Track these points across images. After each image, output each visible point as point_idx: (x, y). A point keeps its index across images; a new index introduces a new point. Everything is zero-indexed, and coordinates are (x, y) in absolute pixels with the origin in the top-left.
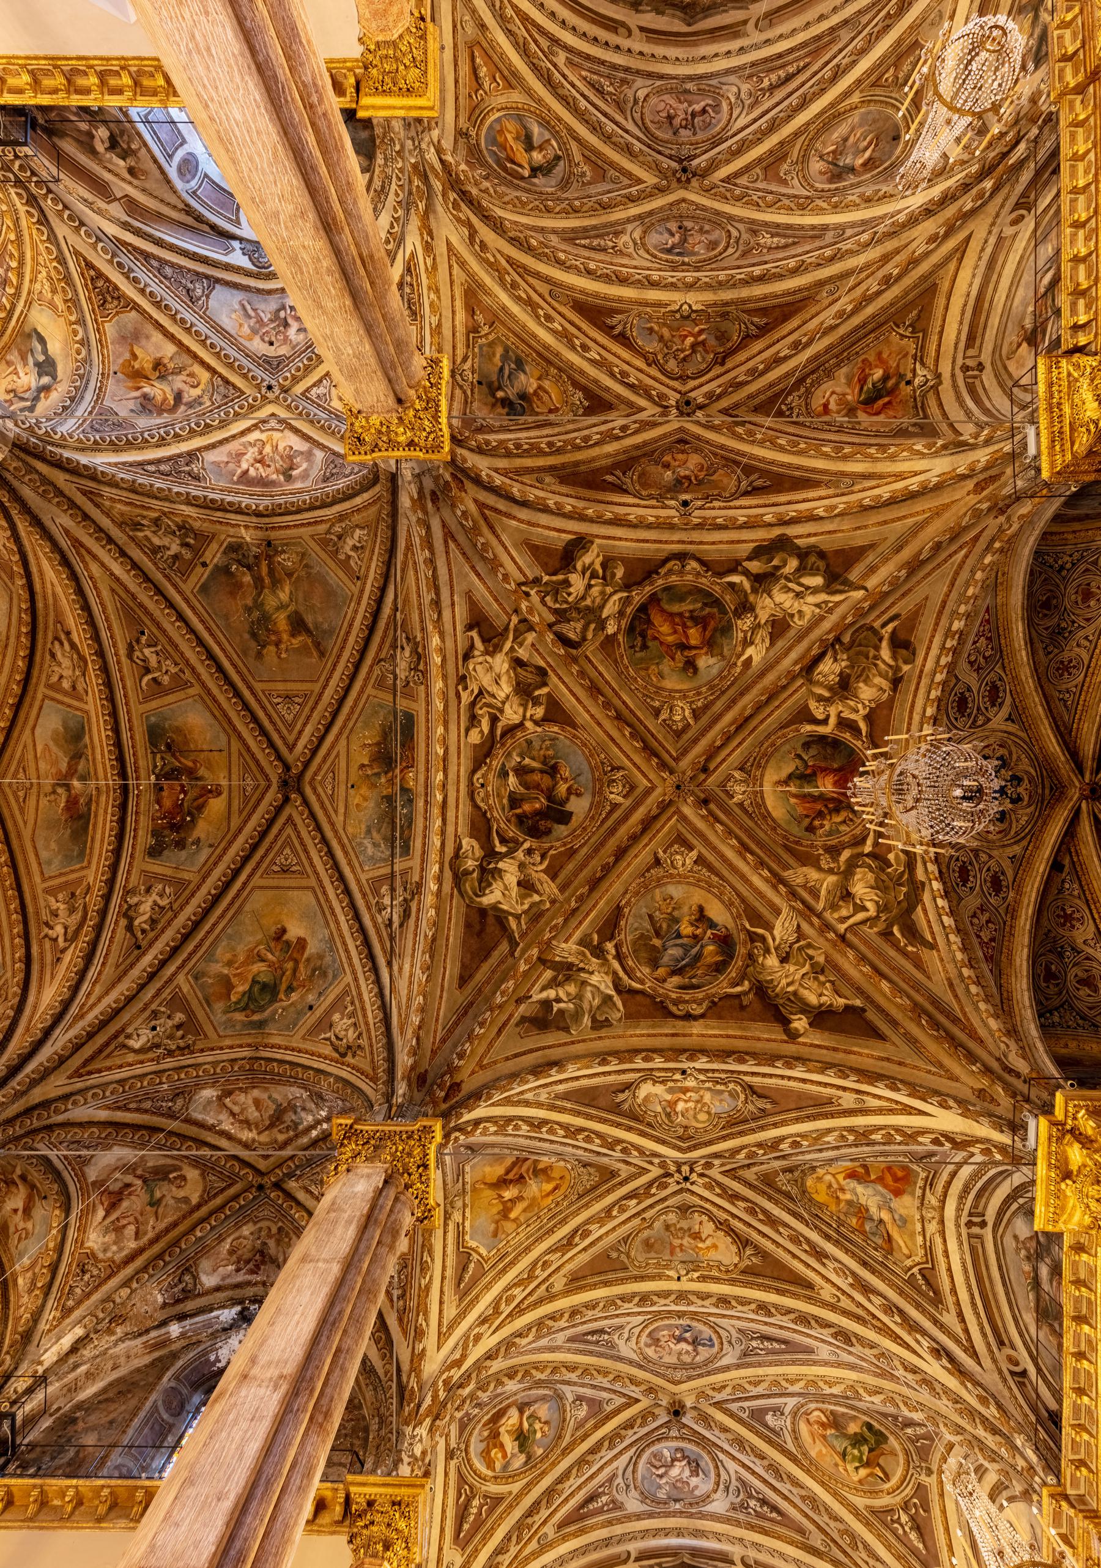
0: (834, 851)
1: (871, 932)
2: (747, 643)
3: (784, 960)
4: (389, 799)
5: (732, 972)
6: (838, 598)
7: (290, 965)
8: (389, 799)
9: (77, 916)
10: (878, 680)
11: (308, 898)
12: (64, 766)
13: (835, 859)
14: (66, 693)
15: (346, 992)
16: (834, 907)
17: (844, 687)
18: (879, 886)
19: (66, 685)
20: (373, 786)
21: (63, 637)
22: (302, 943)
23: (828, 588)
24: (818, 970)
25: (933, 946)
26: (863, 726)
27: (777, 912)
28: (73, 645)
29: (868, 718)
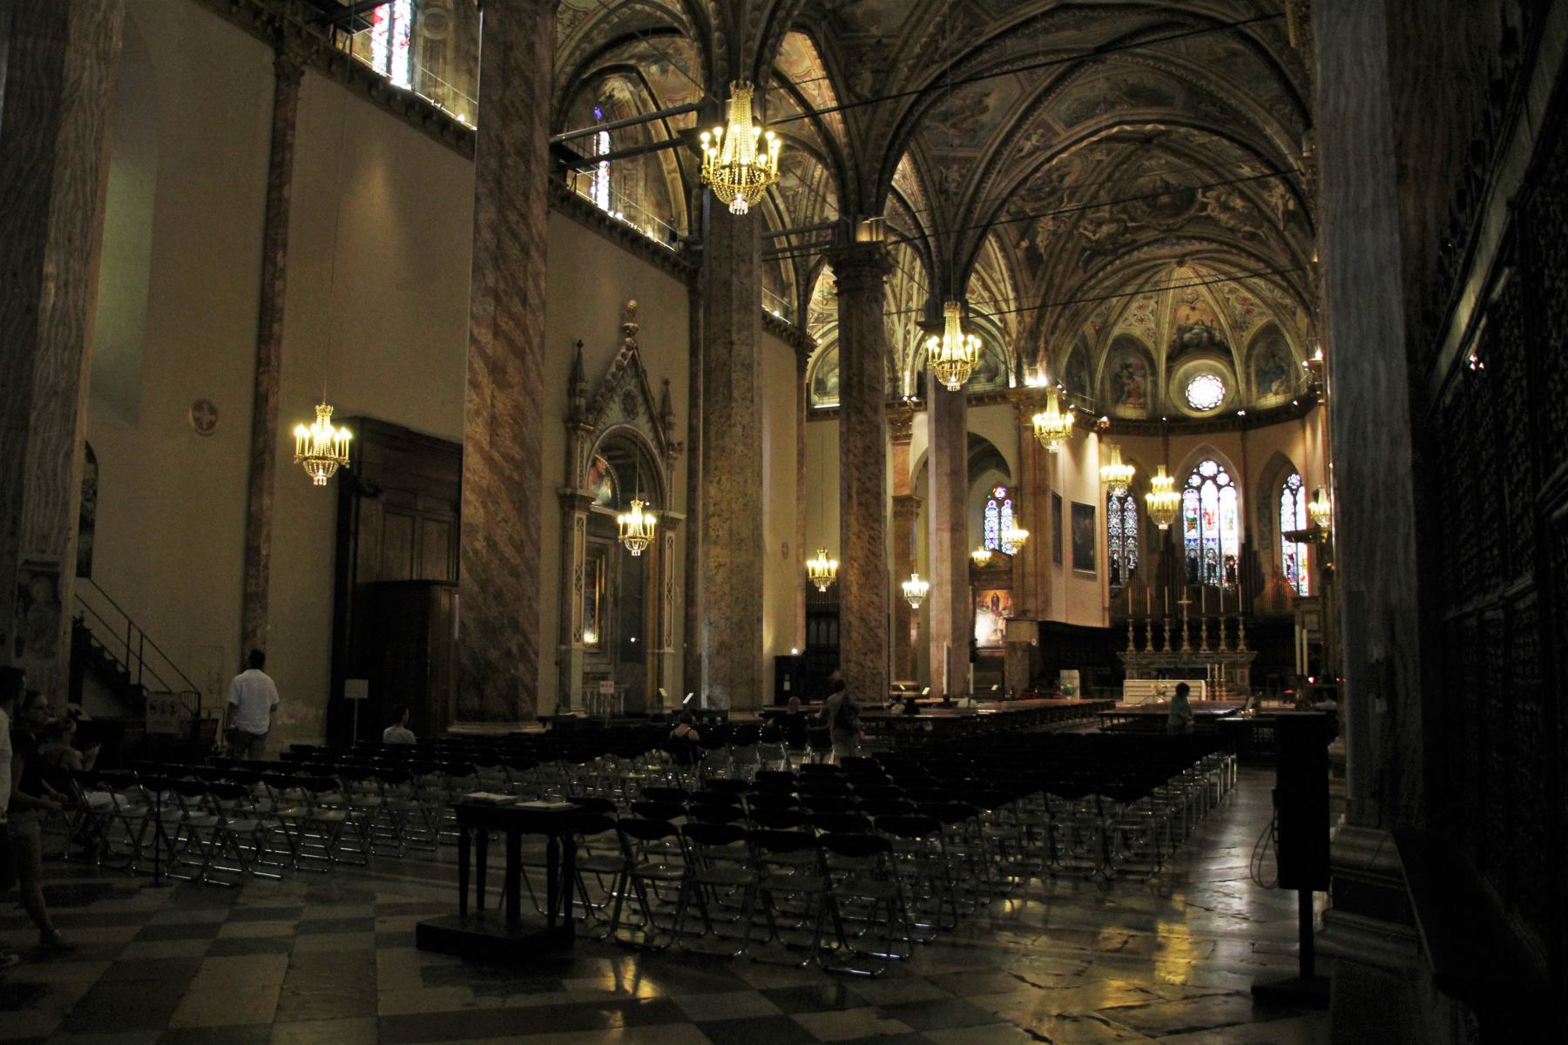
0: (1124, 211)
1: (1084, 243)
2: (1253, 169)
3: (1053, 219)
4: (1105, 100)
5: (1037, 205)
6: (1280, 215)
7: (969, 113)
8: (1105, 100)
10: (1232, 223)
11: (1016, 93)
13: (1120, 212)
15: (970, 160)
16: (1091, 222)
17: (1226, 208)
18: (1110, 236)
20: (1111, 89)
22: (986, 109)
23: (1286, 212)
24: (1054, 233)
25: (1085, 272)
26: (1203, 214)
27: (1079, 201)
29: (1209, 217)
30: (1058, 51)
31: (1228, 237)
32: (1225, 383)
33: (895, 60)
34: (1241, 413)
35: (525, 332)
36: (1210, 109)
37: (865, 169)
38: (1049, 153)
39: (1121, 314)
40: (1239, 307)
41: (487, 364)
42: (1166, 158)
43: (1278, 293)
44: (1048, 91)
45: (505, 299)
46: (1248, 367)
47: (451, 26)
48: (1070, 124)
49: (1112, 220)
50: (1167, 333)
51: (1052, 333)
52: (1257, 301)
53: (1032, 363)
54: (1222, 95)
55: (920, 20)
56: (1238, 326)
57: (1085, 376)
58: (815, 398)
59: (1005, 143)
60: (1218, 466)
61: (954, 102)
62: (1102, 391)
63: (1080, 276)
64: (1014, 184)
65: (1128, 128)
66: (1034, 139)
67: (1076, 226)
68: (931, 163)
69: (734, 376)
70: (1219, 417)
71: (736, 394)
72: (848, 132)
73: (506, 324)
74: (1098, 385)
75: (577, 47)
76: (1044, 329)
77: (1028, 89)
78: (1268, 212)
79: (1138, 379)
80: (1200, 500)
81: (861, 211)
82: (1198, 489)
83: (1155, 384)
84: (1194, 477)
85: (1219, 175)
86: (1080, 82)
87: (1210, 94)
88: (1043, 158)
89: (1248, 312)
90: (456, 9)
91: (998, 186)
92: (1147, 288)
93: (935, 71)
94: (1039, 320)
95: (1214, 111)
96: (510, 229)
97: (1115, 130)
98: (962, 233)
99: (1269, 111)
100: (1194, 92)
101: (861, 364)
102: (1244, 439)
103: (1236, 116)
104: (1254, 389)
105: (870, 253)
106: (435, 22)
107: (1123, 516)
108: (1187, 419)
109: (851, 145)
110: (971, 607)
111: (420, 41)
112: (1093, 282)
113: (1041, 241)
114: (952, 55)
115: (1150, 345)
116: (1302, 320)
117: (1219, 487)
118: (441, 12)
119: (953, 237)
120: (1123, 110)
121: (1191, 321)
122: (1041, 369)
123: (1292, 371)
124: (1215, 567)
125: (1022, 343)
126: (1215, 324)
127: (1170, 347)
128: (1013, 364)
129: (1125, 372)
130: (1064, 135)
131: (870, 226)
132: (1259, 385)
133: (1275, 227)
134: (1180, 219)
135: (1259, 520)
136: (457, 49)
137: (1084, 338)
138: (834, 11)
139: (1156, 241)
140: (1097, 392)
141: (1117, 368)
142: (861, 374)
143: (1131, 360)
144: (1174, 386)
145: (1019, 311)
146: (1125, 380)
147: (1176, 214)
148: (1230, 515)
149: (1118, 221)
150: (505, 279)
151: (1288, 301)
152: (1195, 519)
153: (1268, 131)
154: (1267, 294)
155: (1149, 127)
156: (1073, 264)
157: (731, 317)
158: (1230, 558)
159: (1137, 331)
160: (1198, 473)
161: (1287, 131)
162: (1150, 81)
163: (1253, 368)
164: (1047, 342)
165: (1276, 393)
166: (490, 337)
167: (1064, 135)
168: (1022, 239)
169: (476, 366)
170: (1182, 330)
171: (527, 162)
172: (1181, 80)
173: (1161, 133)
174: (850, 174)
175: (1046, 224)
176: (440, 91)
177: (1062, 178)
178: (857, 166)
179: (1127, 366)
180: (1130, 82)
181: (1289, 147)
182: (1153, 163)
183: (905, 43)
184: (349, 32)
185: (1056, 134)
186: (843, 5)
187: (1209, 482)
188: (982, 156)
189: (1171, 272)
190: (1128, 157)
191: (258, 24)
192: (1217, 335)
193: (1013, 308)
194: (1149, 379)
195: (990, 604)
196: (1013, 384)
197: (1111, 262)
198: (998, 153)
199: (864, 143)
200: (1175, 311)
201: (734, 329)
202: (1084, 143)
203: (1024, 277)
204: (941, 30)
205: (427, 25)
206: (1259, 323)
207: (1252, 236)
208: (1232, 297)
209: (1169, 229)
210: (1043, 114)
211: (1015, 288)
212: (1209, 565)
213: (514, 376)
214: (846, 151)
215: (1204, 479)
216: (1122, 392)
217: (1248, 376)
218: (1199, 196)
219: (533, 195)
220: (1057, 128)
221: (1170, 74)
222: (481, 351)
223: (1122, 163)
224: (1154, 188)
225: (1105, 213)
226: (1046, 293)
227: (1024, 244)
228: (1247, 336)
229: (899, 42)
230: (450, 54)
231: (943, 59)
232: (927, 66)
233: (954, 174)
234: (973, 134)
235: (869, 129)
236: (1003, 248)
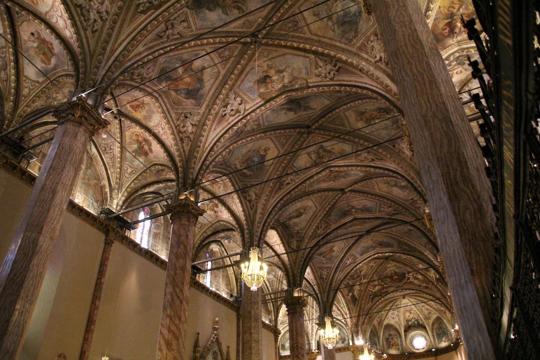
0: (382, 281)
2: (423, 265)
4: (372, 247)
5: (353, 281)
8: (372, 247)
9: (324, 232)
10: (419, 283)
11: (343, 245)
12: (357, 207)
14: (379, 209)
15: (330, 268)
16: (372, 286)
17: (416, 278)
18: (379, 290)
19: (382, 209)
21: (396, 212)
22: (334, 251)
23: (436, 278)
24: (360, 290)
25: (372, 303)
28: (395, 214)
29: (411, 282)
30: (355, 232)
31: (418, 288)
32: (426, 339)
33: (304, 237)
34: (434, 350)
35: (179, 330)
36: (406, 247)
37: (295, 272)
38: (356, 264)
39: (386, 317)
40: (426, 312)
41: (165, 342)
42: (394, 263)
43: (438, 306)
44: (353, 245)
45: (173, 319)
46: (433, 333)
47: (162, 228)
48: (361, 255)
49: (379, 285)
50: (403, 323)
51: (363, 325)
52: (431, 309)
53: (357, 336)
54: (409, 243)
55: (311, 225)
56: (427, 318)
57: (376, 339)
58: (281, 351)
59: (341, 262)
61: (323, 249)
62: (383, 345)
63: (370, 305)
64: (345, 275)
65: (380, 255)
66: (350, 260)
67: (367, 287)
68: (317, 269)
69: (253, 345)
70: (426, 352)
71: (253, 352)
72: (289, 260)
73: (173, 328)
74: (381, 342)
75: (202, 235)
76: (360, 323)
77: (347, 244)
78: (430, 279)
79: (395, 339)
81: (295, 286)
83: (401, 341)
85: (412, 268)
86: (363, 241)
87: (405, 243)
88: (353, 266)
89: (430, 313)
90: (164, 223)
91: (340, 276)
92: (393, 307)
93: (316, 240)
94: (358, 321)
95: (407, 248)
96: (177, 295)
97: (376, 256)
98: (329, 292)
99: (425, 247)
100: (399, 242)
101: (297, 339)
103: (415, 250)
105: (298, 300)
106: (157, 227)
108: (415, 353)
109: (290, 264)
111: (152, 233)
112: (375, 306)
113: (356, 293)
114: (322, 235)
115: (397, 327)
116: (449, 315)
118: (159, 224)
119: (326, 293)
120: (378, 249)
121: (411, 317)
122: (360, 337)
123: (449, 335)
125: (353, 329)
126: (419, 318)
127: (405, 327)
128: (350, 336)
129: (390, 337)
130: (360, 258)
131: (298, 291)
132: (438, 339)
133: (433, 284)
134: (402, 283)
136: (163, 235)
137: (374, 326)
138: (283, 223)
139: (394, 291)
140: (381, 345)
141: (387, 335)
142: (297, 343)
143: (392, 333)
144: (408, 341)
145: (351, 318)
146: (391, 340)
147: (400, 282)
149: (381, 285)
150: (174, 312)
151: (442, 308)
153: (426, 253)
154: (435, 307)
155: (387, 254)
156: (367, 300)
157: (251, 324)
159: (392, 322)
161: (432, 253)
162: (385, 240)
163: (435, 333)
164: (361, 328)
165: (445, 342)
166: (167, 332)
167: (360, 258)
168: (349, 293)
169: (161, 343)
170: (408, 321)
171: (184, 272)
172: (395, 239)
173: (392, 256)
174: (291, 274)
175: (357, 288)
176: (157, 248)
177: (361, 272)
178: (293, 272)
179: (391, 335)
180: (379, 240)
181: (433, 258)
182: (390, 265)
183: (306, 231)
184: (130, 230)
185: (357, 258)
186: (286, 221)
188: (334, 266)
189: (401, 301)
190: (382, 264)
191: (102, 227)
192: (421, 322)
193: (349, 317)
194: (399, 339)
196: (351, 344)
197: (380, 299)
198: (339, 265)
199: (295, 263)
200: (404, 314)
201: (252, 328)
202: (367, 260)
203: (351, 306)
204: (317, 227)
205: (155, 228)
206: (434, 317)
207: (427, 287)
208: (423, 308)
209: (398, 287)
210: (353, 252)
211: (349, 309)
213: (174, 346)
214: (289, 266)
216: (390, 344)
217: (433, 336)
218: (407, 275)
219: (185, 283)
220: (357, 256)
221: (391, 237)
222: (164, 338)
223: (380, 266)
224: (392, 274)
225: (376, 283)
226: (359, 311)
227: (350, 294)
228: (431, 322)
229: (304, 232)
230: (161, 237)
231: (319, 236)
232: (314, 239)
233: (325, 272)
234: (330, 259)
235: (296, 258)
236: (343, 296)
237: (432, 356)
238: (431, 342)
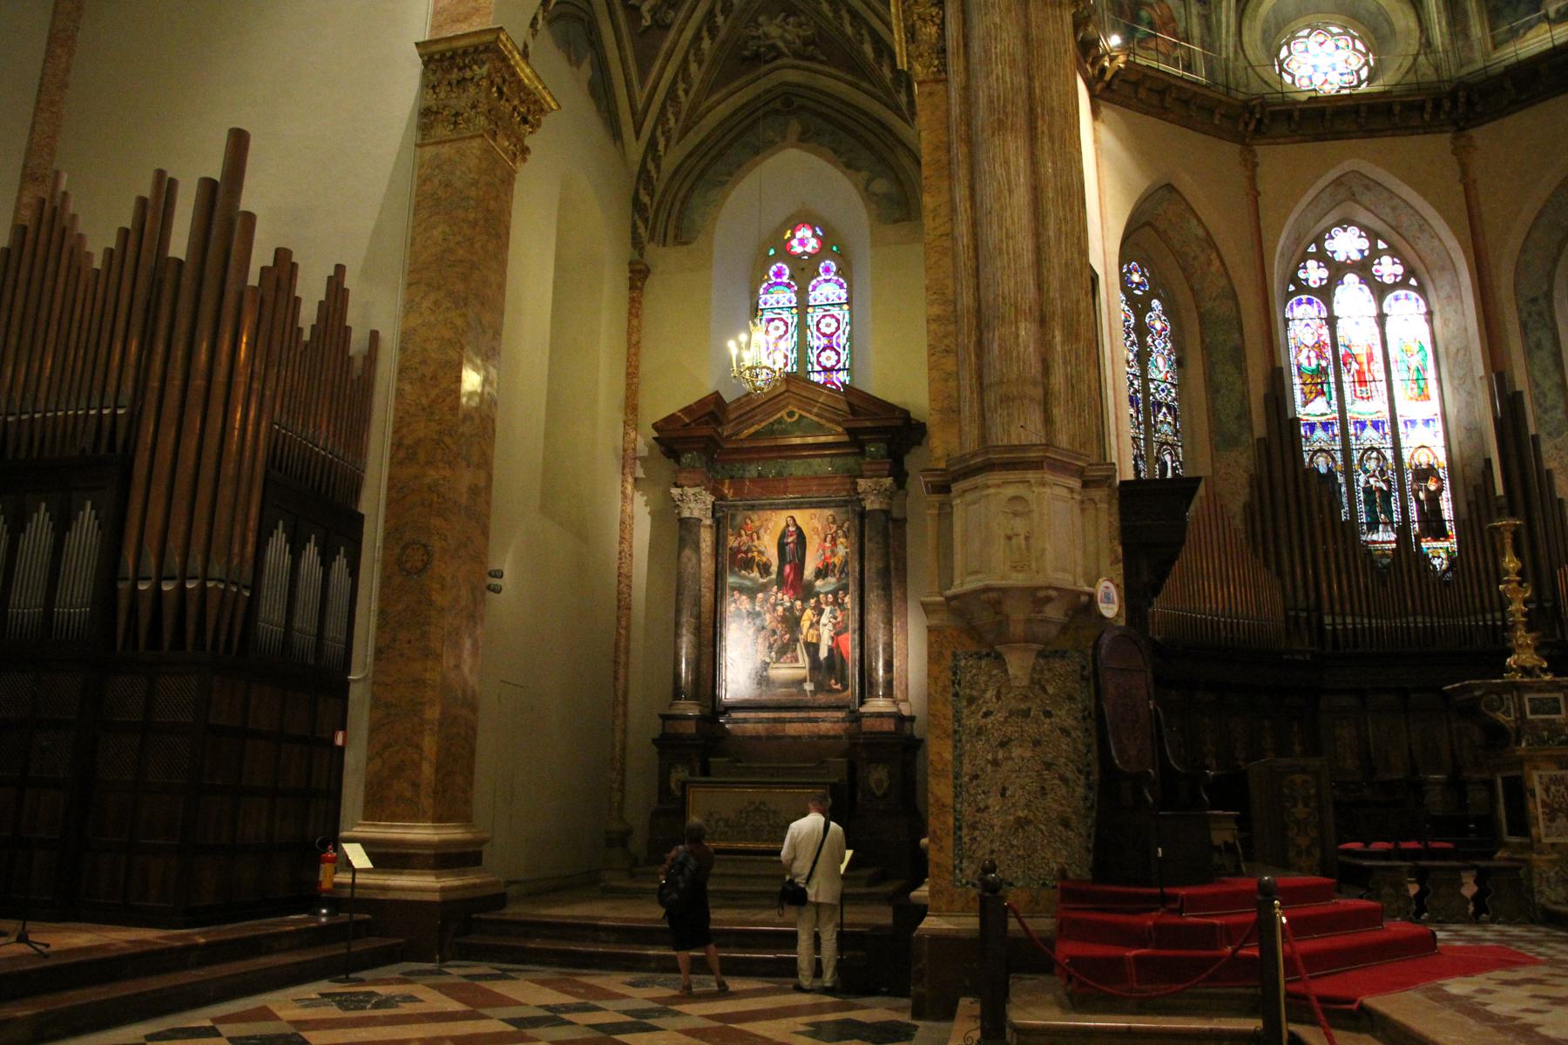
60: (1372, 235)
80: (1331, 322)
82: (1325, 293)
84: (1311, 264)
102: (1462, 152)
104: (1477, 29)
107: (1142, 343)
110: (707, 565)
117: (1380, 291)
124: (1386, 496)
135: (1528, 354)
148: (1415, 362)
152: (1322, 371)
158: (1425, 473)
160: (1324, 258)
187: (1351, 279)
195: (772, 554)
212: (1369, 491)
215: (1337, 270)
237: (1427, 129)
238: (1427, 44)
